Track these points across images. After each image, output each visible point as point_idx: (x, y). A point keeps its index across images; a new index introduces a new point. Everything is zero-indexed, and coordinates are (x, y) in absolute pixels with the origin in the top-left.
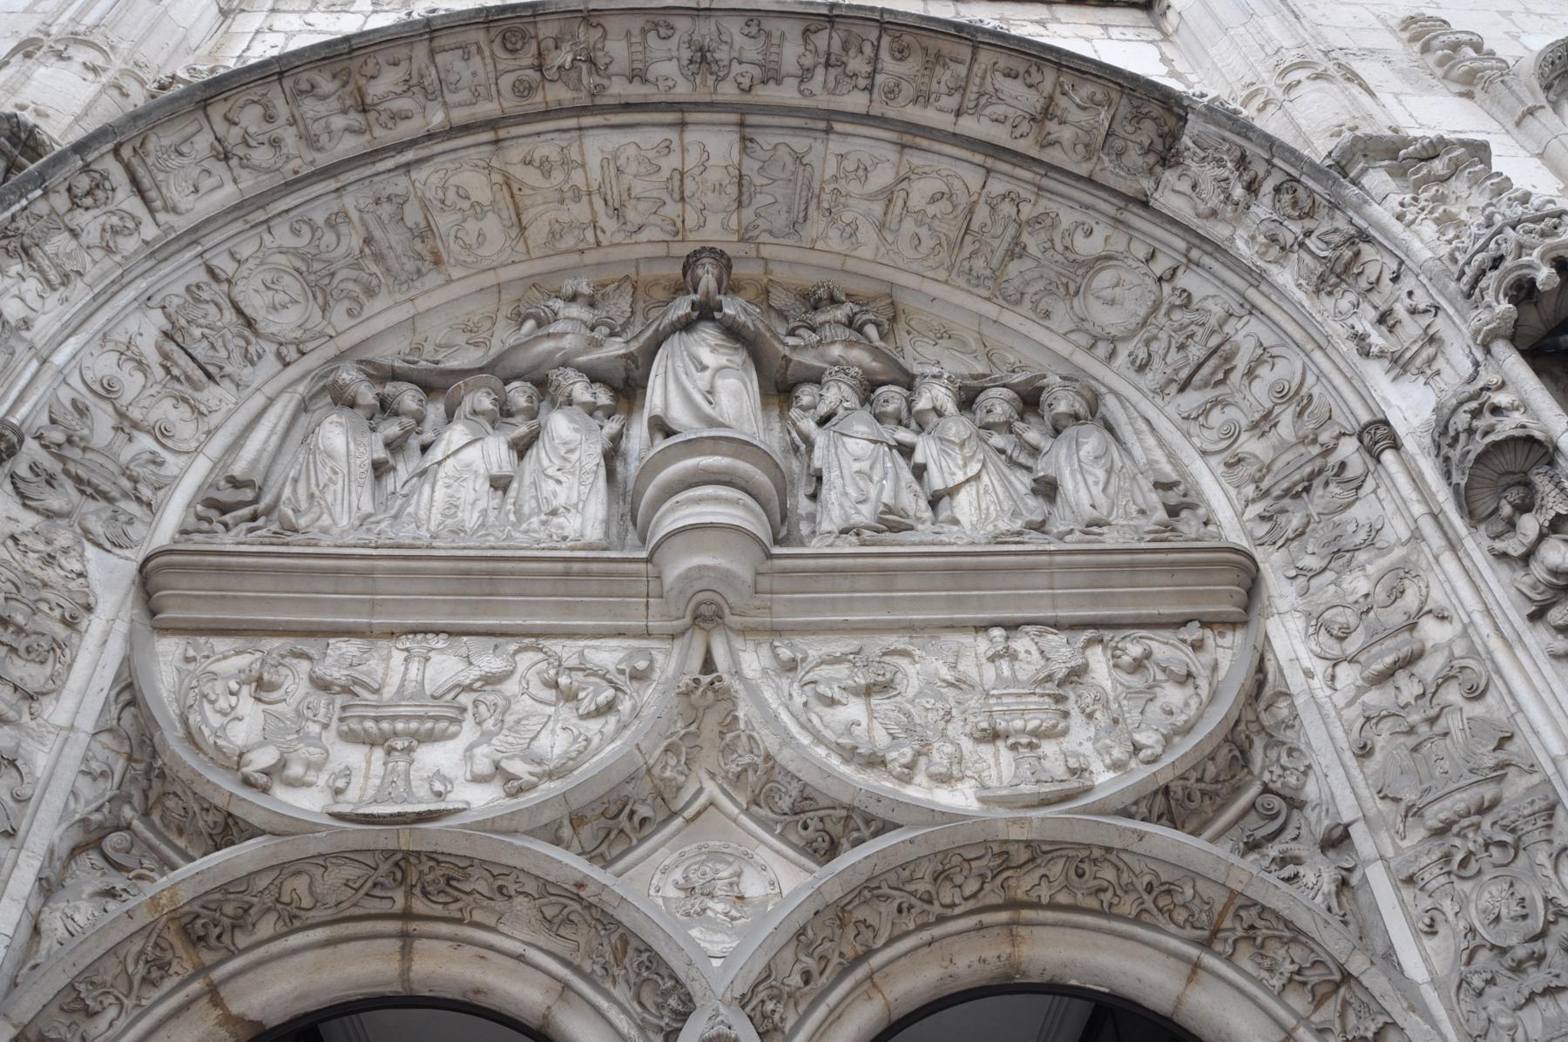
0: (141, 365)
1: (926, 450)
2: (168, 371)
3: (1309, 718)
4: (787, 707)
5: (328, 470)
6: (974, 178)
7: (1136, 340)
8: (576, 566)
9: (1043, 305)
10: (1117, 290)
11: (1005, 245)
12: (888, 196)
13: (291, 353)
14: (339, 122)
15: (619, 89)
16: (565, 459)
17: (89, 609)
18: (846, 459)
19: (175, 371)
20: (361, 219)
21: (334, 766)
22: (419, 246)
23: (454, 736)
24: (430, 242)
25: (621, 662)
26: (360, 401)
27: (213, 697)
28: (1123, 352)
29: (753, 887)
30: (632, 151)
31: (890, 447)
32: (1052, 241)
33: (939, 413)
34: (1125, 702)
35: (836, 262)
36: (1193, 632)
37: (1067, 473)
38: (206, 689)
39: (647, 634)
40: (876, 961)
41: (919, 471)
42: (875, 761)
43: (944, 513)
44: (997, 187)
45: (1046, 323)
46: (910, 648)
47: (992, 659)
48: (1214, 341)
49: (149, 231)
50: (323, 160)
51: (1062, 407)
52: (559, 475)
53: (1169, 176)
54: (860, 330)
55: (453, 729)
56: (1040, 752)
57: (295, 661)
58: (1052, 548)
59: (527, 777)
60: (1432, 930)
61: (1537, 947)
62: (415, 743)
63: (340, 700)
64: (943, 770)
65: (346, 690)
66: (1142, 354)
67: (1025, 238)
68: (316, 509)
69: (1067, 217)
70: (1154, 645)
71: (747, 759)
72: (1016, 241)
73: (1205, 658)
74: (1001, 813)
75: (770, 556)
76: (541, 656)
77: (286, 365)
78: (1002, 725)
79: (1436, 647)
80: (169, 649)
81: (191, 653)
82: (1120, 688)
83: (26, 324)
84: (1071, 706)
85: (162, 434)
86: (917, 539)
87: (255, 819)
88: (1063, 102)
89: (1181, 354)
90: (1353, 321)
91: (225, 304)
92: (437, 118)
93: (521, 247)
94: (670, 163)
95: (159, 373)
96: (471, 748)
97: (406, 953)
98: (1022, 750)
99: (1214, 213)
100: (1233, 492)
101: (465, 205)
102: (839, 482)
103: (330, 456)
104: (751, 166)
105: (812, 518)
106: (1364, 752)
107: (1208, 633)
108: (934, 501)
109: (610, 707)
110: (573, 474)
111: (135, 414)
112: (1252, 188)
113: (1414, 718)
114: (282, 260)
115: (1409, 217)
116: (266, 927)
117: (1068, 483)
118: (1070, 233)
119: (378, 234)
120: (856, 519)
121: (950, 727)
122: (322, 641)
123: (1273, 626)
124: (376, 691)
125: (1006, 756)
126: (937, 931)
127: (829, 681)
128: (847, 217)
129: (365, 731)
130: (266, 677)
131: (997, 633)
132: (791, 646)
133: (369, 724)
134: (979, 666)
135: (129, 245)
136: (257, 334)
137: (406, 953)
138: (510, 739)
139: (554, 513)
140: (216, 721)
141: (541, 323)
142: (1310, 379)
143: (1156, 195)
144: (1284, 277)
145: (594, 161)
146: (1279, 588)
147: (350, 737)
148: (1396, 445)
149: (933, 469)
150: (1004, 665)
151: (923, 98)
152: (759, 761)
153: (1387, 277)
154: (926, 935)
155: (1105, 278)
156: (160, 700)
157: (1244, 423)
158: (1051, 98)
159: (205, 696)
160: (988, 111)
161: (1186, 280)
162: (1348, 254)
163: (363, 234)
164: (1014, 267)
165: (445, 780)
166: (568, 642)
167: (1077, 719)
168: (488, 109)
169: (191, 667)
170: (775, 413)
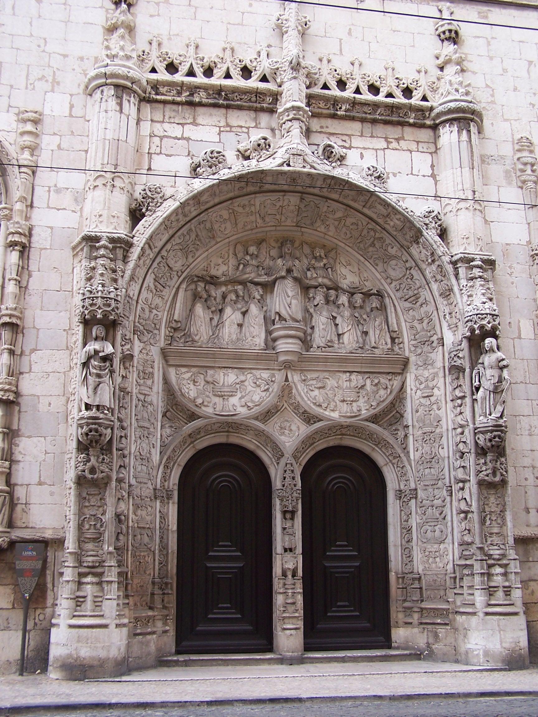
0: (151, 291)
1: (339, 320)
2: (156, 290)
3: (409, 400)
6: (365, 224)
8: (260, 354)
9: (376, 262)
12: (340, 220)
13: (180, 274)
14: (193, 209)
15: (267, 187)
17: (154, 362)
19: (158, 290)
21: (213, 402)
22: (210, 234)
26: (203, 297)
29: (294, 428)
30: (269, 201)
33: (344, 306)
35: (322, 235)
37: (371, 330)
38: (183, 382)
39: (274, 369)
40: (315, 444)
41: (336, 325)
42: (320, 406)
43: (341, 341)
44: (370, 226)
45: (376, 267)
48: (416, 292)
49: (152, 256)
50: (188, 219)
51: (374, 305)
53: (415, 246)
58: (363, 355)
60: (417, 451)
61: (431, 460)
63: (212, 386)
65: (212, 383)
66: (398, 288)
67: (375, 242)
68: (199, 335)
69: (388, 241)
71: (294, 401)
72: (373, 243)
73: (391, 383)
74: (343, 420)
75: (302, 354)
77: (179, 277)
78: (345, 399)
79: (436, 396)
80: (172, 372)
81: (178, 373)
83: (134, 295)
84: (360, 394)
85: (156, 308)
86: (334, 351)
87: (200, 415)
88: (393, 216)
90: (445, 308)
91: (165, 265)
92: (217, 200)
93: (235, 229)
94: (278, 204)
95: (154, 291)
96: (240, 398)
97: (228, 436)
99: (423, 261)
100: (409, 335)
101: (222, 220)
102: (318, 332)
103: (200, 318)
104: (302, 206)
106: (417, 411)
107: (393, 376)
109: (267, 390)
111: (153, 306)
112: (433, 261)
113: (427, 409)
114: (176, 247)
115: (463, 292)
116: (202, 434)
117: (371, 333)
119: (199, 234)
120: (322, 345)
123: (408, 375)
125: (345, 405)
126: (327, 439)
128: (327, 223)
131: (348, 374)
132: (305, 376)
133: (219, 393)
135: (148, 262)
136: (172, 271)
137: (228, 436)
140: (187, 391)
142: (433, 315)
143: (411, 248)
144: (435, 286)
145: (258, 204)
146: (412, 367)
148: (443, 345)
149: (340, 326)
150: (348, 383)
151: (355, 200)
153: (454, 304)
154: (325, 440)
155: (393, 262)
157: (417, 318)
158: (389, 213)
160: (372, 209)
161: (413, 271)
162: (448, 294)
164: (371, 249)
165: (236, 406)
166: (257, 371)
168: (231, 195)
169: (178, 376)
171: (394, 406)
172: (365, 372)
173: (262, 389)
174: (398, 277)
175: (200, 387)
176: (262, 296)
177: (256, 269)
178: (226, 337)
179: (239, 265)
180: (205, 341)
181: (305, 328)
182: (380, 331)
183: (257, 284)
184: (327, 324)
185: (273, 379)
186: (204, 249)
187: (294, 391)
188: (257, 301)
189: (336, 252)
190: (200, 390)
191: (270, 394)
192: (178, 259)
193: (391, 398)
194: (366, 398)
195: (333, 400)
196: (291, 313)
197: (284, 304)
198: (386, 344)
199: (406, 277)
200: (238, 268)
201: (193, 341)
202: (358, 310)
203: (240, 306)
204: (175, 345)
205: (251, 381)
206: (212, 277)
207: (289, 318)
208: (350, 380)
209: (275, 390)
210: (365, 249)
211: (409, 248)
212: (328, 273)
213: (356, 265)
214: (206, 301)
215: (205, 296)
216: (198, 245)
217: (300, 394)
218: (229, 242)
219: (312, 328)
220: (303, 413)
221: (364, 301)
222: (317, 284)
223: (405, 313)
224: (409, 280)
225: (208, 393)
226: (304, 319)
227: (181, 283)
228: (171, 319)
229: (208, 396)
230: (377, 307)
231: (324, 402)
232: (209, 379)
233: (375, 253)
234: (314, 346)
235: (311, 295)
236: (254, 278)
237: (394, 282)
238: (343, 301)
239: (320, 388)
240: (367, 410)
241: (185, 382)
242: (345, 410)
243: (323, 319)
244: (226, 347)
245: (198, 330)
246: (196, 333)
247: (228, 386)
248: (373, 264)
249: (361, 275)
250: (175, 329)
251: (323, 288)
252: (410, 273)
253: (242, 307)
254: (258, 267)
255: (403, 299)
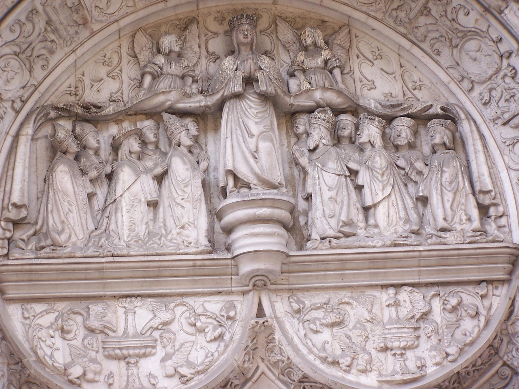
1: (363, 178)
4: (297, 334)
5: (66, 203)
7: (485, 85)
8: (198, 263)
9: (436, 46)
10: (478, 53)
11: (418, 8)
13: (18, 105)
16: (184, 191)
18: (325, 188)
20: (44, 10)
21: (106, 372)
22: (75, 17)
23: (154, 354)
24: (81, 12)
25: (221, 311)
27: (44, 339)
28: (478, 89)
31: (346, 176)
32: (446, 12)
33: (373, 146)
34: (445, 330)
36: (482, 290)
37: (434, 192)
38: (40, 335)
41: (359, 188)
42: (335, 363)
43: (371, 221)
45: (437, 58)
46: (351, 301)
47: (388, 306)
51: (437, 140)
52: (183, 203)
54: (331, 72)
55: (154, 351)
56: (405, 357)
57: (75, 316)
58: (421, 248)
59: (190, 376)
62: (138, 359)
63: (101, 337)
64: (363, 368)
65: (102, 332)
66: (486, 97)
67: (430, 5)
68: (67, 231)
70: (463, 295)
71: (279, 357)
73: (487, 303)
75: (288, 256)
76: (185, 308)
77: (18, 112)
78: (390, 345)
81: (26, 315)
82: (444, 322)
84: (421, 332)
86: (357, 244)
89: (506, 104)
96: (163, 360)
98: (397, 356)
102: (320, 207)
103: (66, 194)
105: (306, 213)
107: (490, 287)
108: (366, 209)
109: (220, 338)
110: (189, 201)
114: (7, 50)
118: (456, 10)
119: (54, 17)
120: (331, 233)
121: (367, 344)
122: (84, 304)
124: (114, 332)
125: (390, 358)
127: (316, 318)
129: (116, 354)
130: (65, 328)
131: (391, 291)
132: (298, 302)
133: (117, 351)
134: (382, 309)
138: (179, 356)
139: (183, 227)
140: (48, 351)
141: (155, 77)
147: (110, 357)
149: (366, 191)
150: (393, 309)
152: (285, 359)
155: (472, 45)
156: (19, 341)
159: (40, 338)
163: (45, 18)
164: (422, 20)
165: (155, 377)
166: (196, 299)
167: (423, 339)
169: (28, 322)
170: (284, 132)
171: (497, 353)
172: (427, 285)
173: (210, 335)
174: (486, 76)
175: (77, 343)
176: (196, 139)
177: (179, 82)
178: (125, 232)
179: (143, 76)
180: (80, 244)
181: (292, 200)
182: (455, 194)
183: (183, 114)
184: (338, 187)
185: (232, 314)
186: (67, 50)
187: (278, 335)
188: (185, 151)
189: (349, 32)
190: (76, 348)
191: (226, 346)
192: (11, 74)
193: (488, 335)
194: (434, 340)
195: (364, 350)
196: (258, 171)
197: (243, 153)
198: (469, 219)
199: (501, 74)
200: (141, 84)
201: (55, 245)
202: (405, 152)
203: (149, 164)
204: (17, 256)
205: (183, 320)
206: (86, 107)
207: (255, 182)
208: (397, 304)
209: (237, 337)
210: (410, 22)
211: (501, 12)
212: (334, 77)
213: (394, 57)
214: (77, 158)
215: (74, 148)
216: (53, 41)
217: (290, 342)
218: (120, 30)
219: (308, 198)
220: (300, 382)
221: (416, 133)
222: (313, 104)
223: (506, 151)
224: (508, 80)
225: (93, 354)
226: (290, 182)
227: (22, 125)
228: (6, 202)
229: (94, 361)
230: (444, 144)
231: (343, 356)
232: (94, 323)
233: (430, 28)
234: (315, 236)
235: (301, 129)
236: (178, 102)
237: (476, 86)
238: (369, 135)
239: (333, 325)
240: (437, 364)
241: (43, 334)
242: (390, 368)
243: (330, 179)
244: (125, 252)
245: (63, 222)
246: (60, 228)
247: (136, 335)
248: (429, 51)
249: (406, 78)
250: (16, 224)
251: (325, 112)
252: (509, 65)
253: (156, 165)
254: (183, 77)
255: (500, 122)
